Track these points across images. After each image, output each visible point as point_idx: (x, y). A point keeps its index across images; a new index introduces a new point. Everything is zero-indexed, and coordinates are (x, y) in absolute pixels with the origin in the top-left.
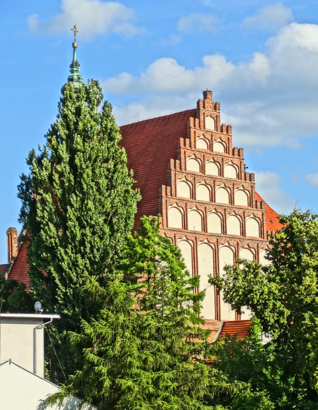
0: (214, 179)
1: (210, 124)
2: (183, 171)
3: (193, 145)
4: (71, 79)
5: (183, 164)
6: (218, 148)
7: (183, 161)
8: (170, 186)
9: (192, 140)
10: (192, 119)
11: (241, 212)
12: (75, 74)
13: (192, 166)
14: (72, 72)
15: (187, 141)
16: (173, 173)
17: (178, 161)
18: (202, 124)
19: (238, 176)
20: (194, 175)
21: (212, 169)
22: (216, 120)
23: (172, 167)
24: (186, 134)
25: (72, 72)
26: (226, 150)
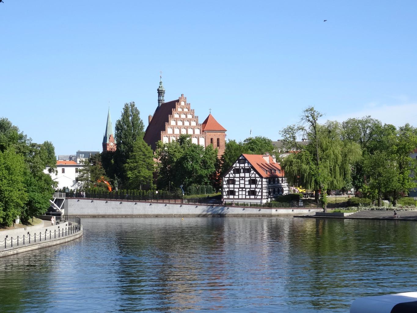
0: (184, 119)
1: (183, 103)
2: (173, 118)
3: (176, 110)
4: (160, 87)
5: (173, 116)
6: (186, 110)
7: (173, 115)
8: (168, 122)
9: (176, 109)
10: (176, 103)
11: (193, 127)
12: (161, 85)
13: (176, 116)
14: (160, 85)
15: (175, 109)
16: (169, 119)
17: (171, 115)
18: (180, 104)
19: (193, 117)
20: (176, 118)
21: (183, 116)
22: (185, 102)
23: (169, 117)
24: (174, 107)
25: (160, 85)
26: (189, 110)
